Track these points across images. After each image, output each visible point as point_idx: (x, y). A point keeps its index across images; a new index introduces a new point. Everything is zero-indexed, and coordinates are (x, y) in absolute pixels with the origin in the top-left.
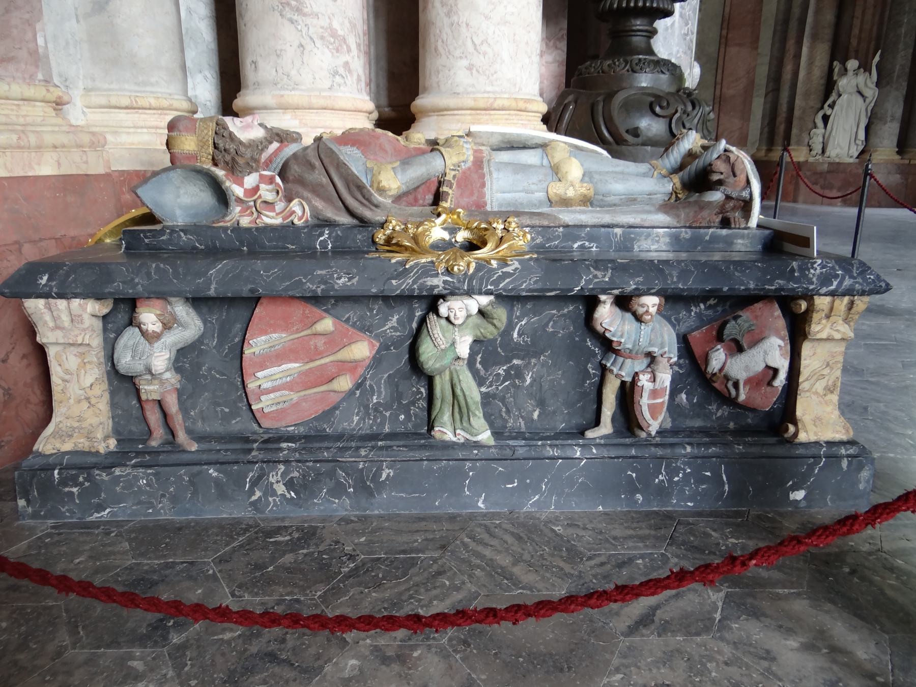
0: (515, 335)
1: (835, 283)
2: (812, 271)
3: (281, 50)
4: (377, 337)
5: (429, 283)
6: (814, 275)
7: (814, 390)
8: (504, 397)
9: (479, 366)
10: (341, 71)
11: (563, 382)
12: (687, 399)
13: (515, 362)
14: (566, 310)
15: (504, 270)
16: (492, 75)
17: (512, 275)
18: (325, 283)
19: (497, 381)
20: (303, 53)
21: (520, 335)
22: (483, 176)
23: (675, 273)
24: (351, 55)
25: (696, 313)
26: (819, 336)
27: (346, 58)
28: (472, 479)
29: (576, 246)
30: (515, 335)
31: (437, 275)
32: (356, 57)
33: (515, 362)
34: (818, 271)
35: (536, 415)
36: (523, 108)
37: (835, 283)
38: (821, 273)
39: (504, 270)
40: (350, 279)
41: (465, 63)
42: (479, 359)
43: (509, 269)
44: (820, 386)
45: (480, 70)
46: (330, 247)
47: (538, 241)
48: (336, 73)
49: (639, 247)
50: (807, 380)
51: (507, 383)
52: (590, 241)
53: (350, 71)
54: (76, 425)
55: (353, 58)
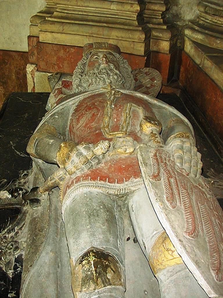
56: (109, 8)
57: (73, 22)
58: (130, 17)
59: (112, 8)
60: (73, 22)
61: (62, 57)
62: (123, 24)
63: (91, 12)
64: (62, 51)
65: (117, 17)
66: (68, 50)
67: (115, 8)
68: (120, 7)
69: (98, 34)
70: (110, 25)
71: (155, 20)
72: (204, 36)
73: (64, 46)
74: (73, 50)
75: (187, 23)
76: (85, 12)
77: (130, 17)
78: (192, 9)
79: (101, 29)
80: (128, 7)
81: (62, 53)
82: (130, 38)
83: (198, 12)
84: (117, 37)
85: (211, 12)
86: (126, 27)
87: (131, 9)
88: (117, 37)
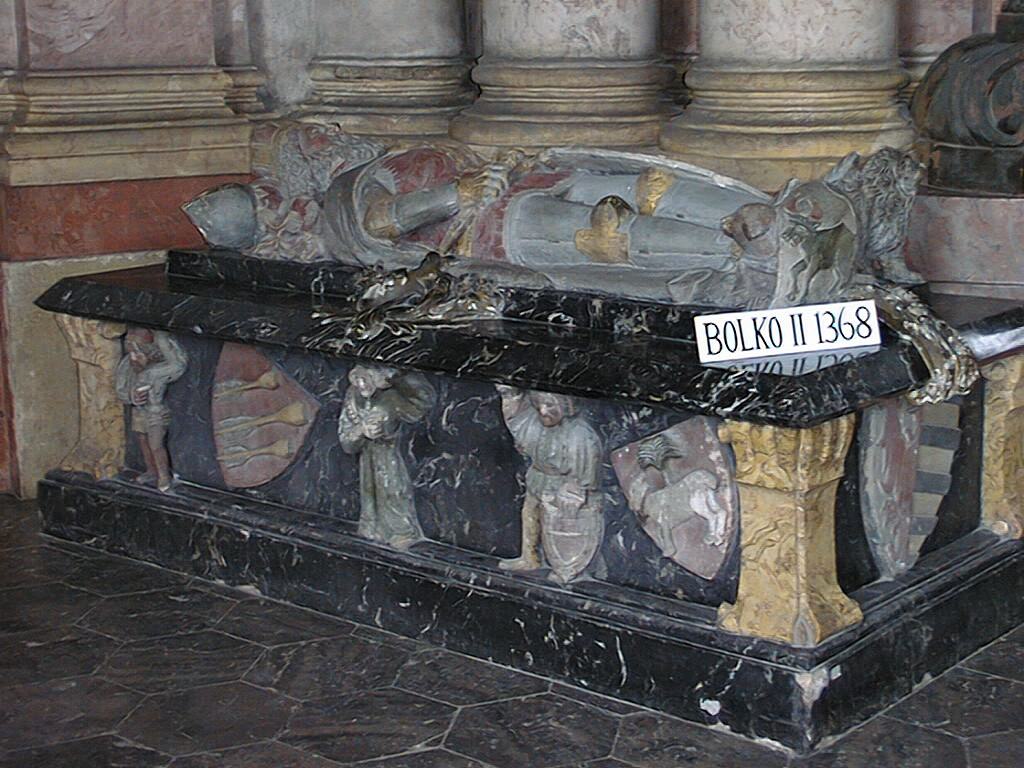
0: (444, 422)
1: (737, 404)
2: (721, 384)
3: (505, 8)
4: (321, 400)
5: (331, 345)
6: (719, 389)
7: (761, 561)
8: (435, 497)
9: (411, 453)
10: (583, 31)
11: (492, 491)
12: (624, 541)
13: (445, 455)
14: (490, 399)
15: (404, 339)
16: (755, 38)
17: (407, 344)
18: (251, 331)
19: (428, 476)
20: (527, 10)
21: (448, 422)
22: (501, 215)
23: (564, 367)
24: (603, 6)
25: (628, 425)
26: (745, 480)
27: (595, 11)
28: (371, 583)
29: (551, 318)
30: (444, 422)
31: (341, 337)
32: (614, 10)
33: (445, 455)
34: (728, 385)
35: (467, 527)
36: (800, 88)
37: (737, 404)
38: (730, 388)
39: (404, 339)
40: (273, 329)
41: (721, 20)
42: (411, 446)
43: (407, 340)
44: (770, 556)
45: (738, 30)
46: (322, 290)
47: (512, 307)
48: (574, 34)
49: (620, 327)
50: (750, 544)
51: (437, 481)
52: (567, 314)
53: (600, 31)
54: (92, 446)
55: (607, 9)
56: (164, 88)
57: (88, 128)
58: (211, 102)
59: (170, 89)
60: (88, 128)
61: (77, 212)
62: (203, 117)
63: (119, 105)
64: (77, 199)
65: (181, 105)
66: (91, 194)
67: (178, 88)
68: (189, 84)
69: (159, 145)
70: (178, 123)
71: (247, 106)
72: (360, 118)
73: (81, 187)
74: (104, 191)
75: (295, 108)
76: (103, 105)
77: (211, 102)
78: (297, 79)
79: (164, 132)
80: (207, 82)
81: (76, 204)
82: (233, 141)
83: (311, 82)
84: (203, 143)
85: (351, 74)
86: (216, 122)
87: (215, 84)
88: (203, 143)
